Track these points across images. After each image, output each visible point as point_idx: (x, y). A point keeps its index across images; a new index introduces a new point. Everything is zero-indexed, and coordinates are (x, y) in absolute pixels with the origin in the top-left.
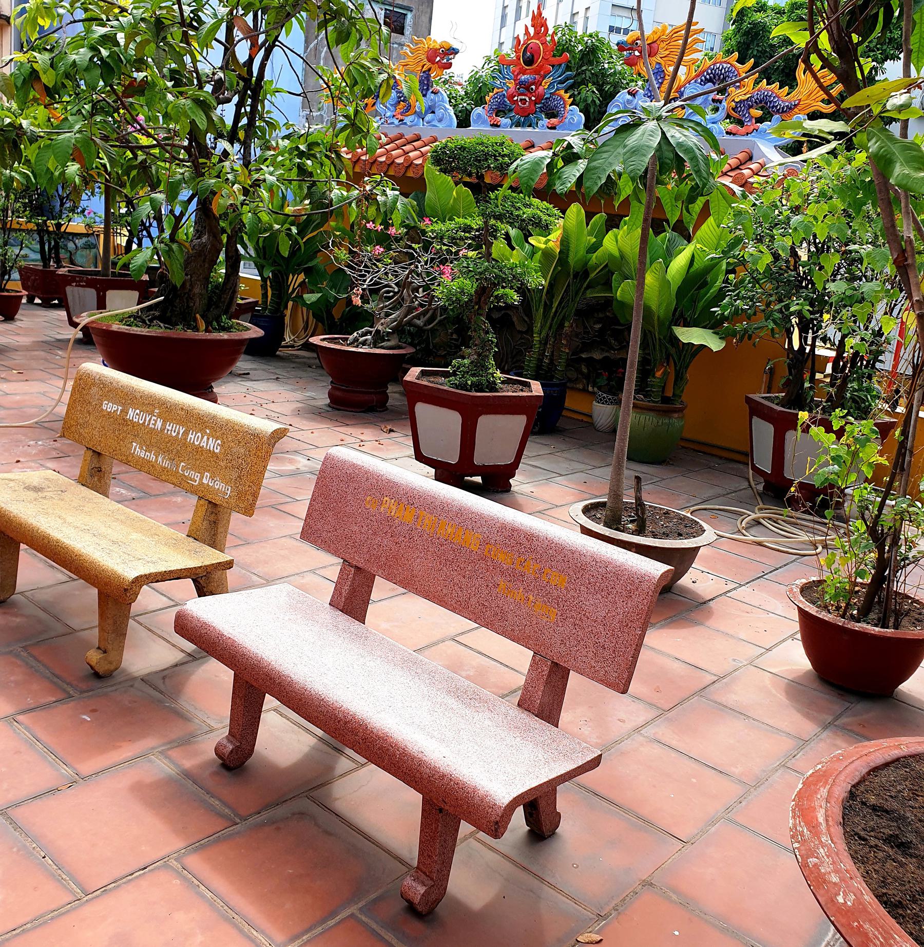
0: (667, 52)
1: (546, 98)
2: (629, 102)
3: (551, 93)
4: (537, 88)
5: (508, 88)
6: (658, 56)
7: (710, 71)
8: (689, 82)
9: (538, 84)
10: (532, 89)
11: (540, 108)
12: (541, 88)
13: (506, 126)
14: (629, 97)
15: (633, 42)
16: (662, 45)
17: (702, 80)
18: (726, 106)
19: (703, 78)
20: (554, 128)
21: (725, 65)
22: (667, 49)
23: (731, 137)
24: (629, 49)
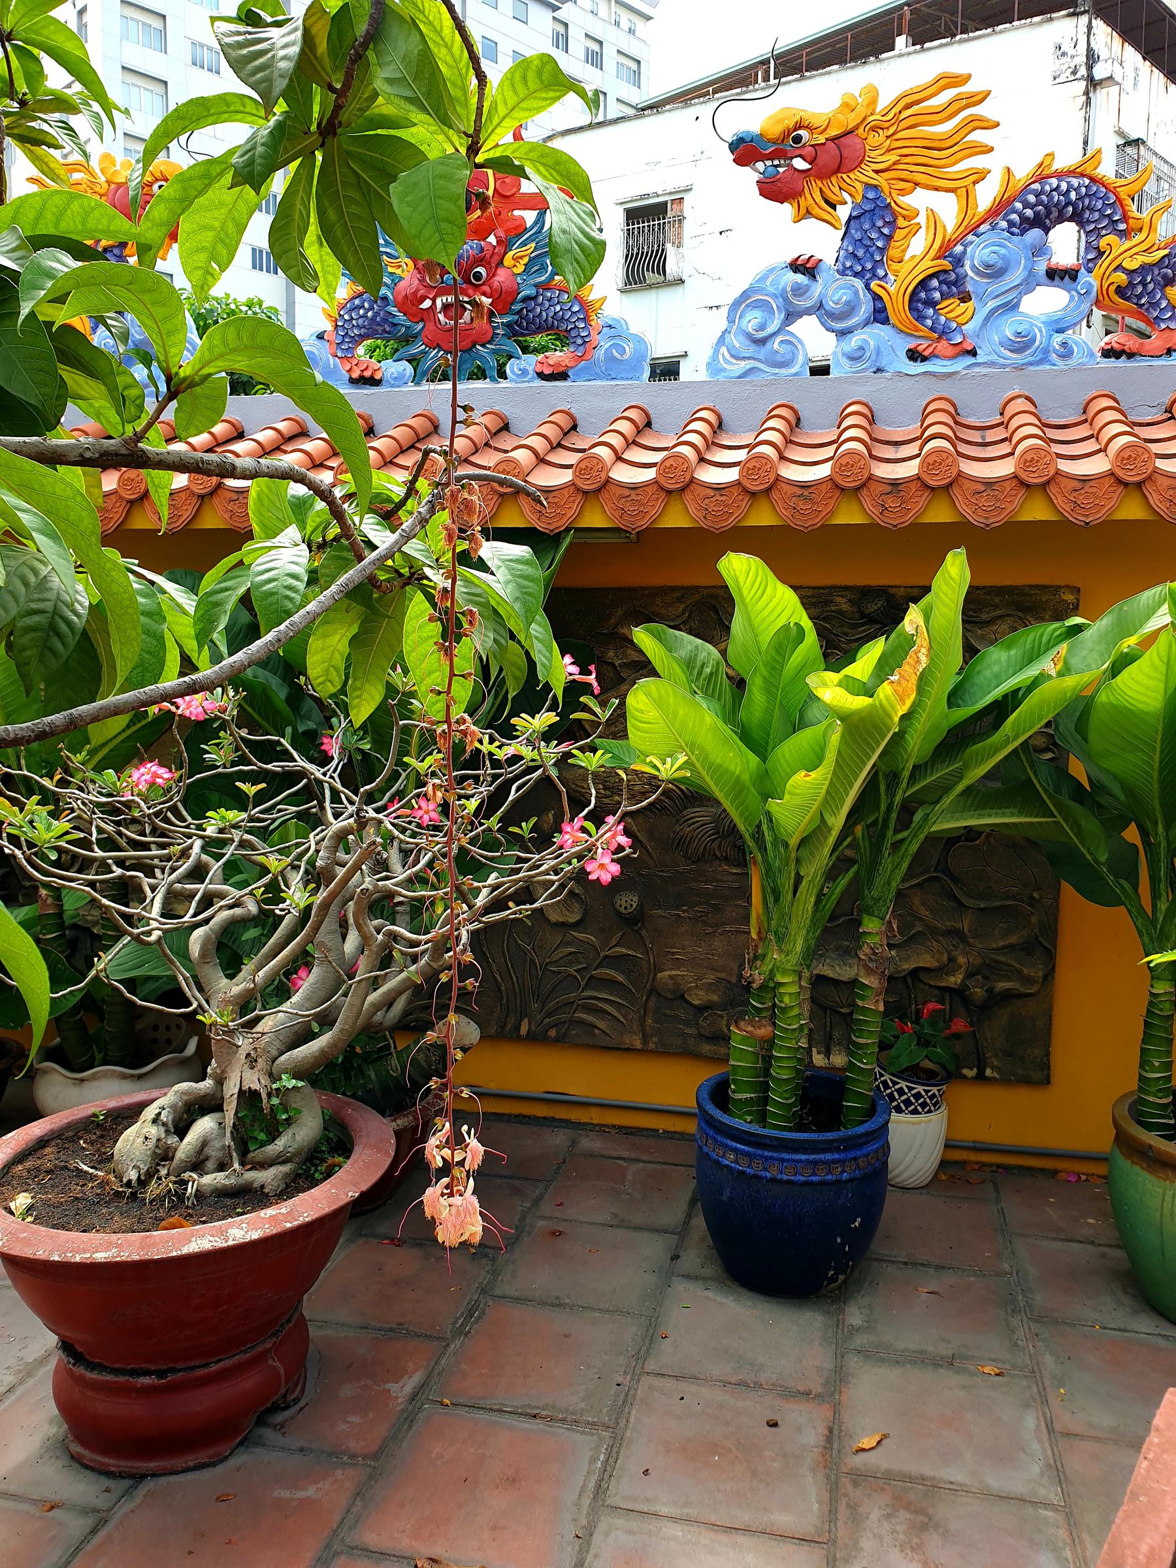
0: (893, 157)
1: (527, 299)
2: (798, 291)
3: (537, 286)
4: (492, 275)
5: (396, 280)
6: (868, 169)
7: (1032, 198)
8: (974, 230)
9: (493, 261)
10: (478, 276)
11: (508, 325)
12: (500, 271)
13: (399, 380)
14: (800, 278)
15: (786, 134)
16: (874, 139)
17: (1011, 224)
18: (1096, 284)
19: (1014, 217)
20: (562, 376)
21: (1075, 182)
22: (889, 150)
23: (1122, 362)
24: (771, 157)
